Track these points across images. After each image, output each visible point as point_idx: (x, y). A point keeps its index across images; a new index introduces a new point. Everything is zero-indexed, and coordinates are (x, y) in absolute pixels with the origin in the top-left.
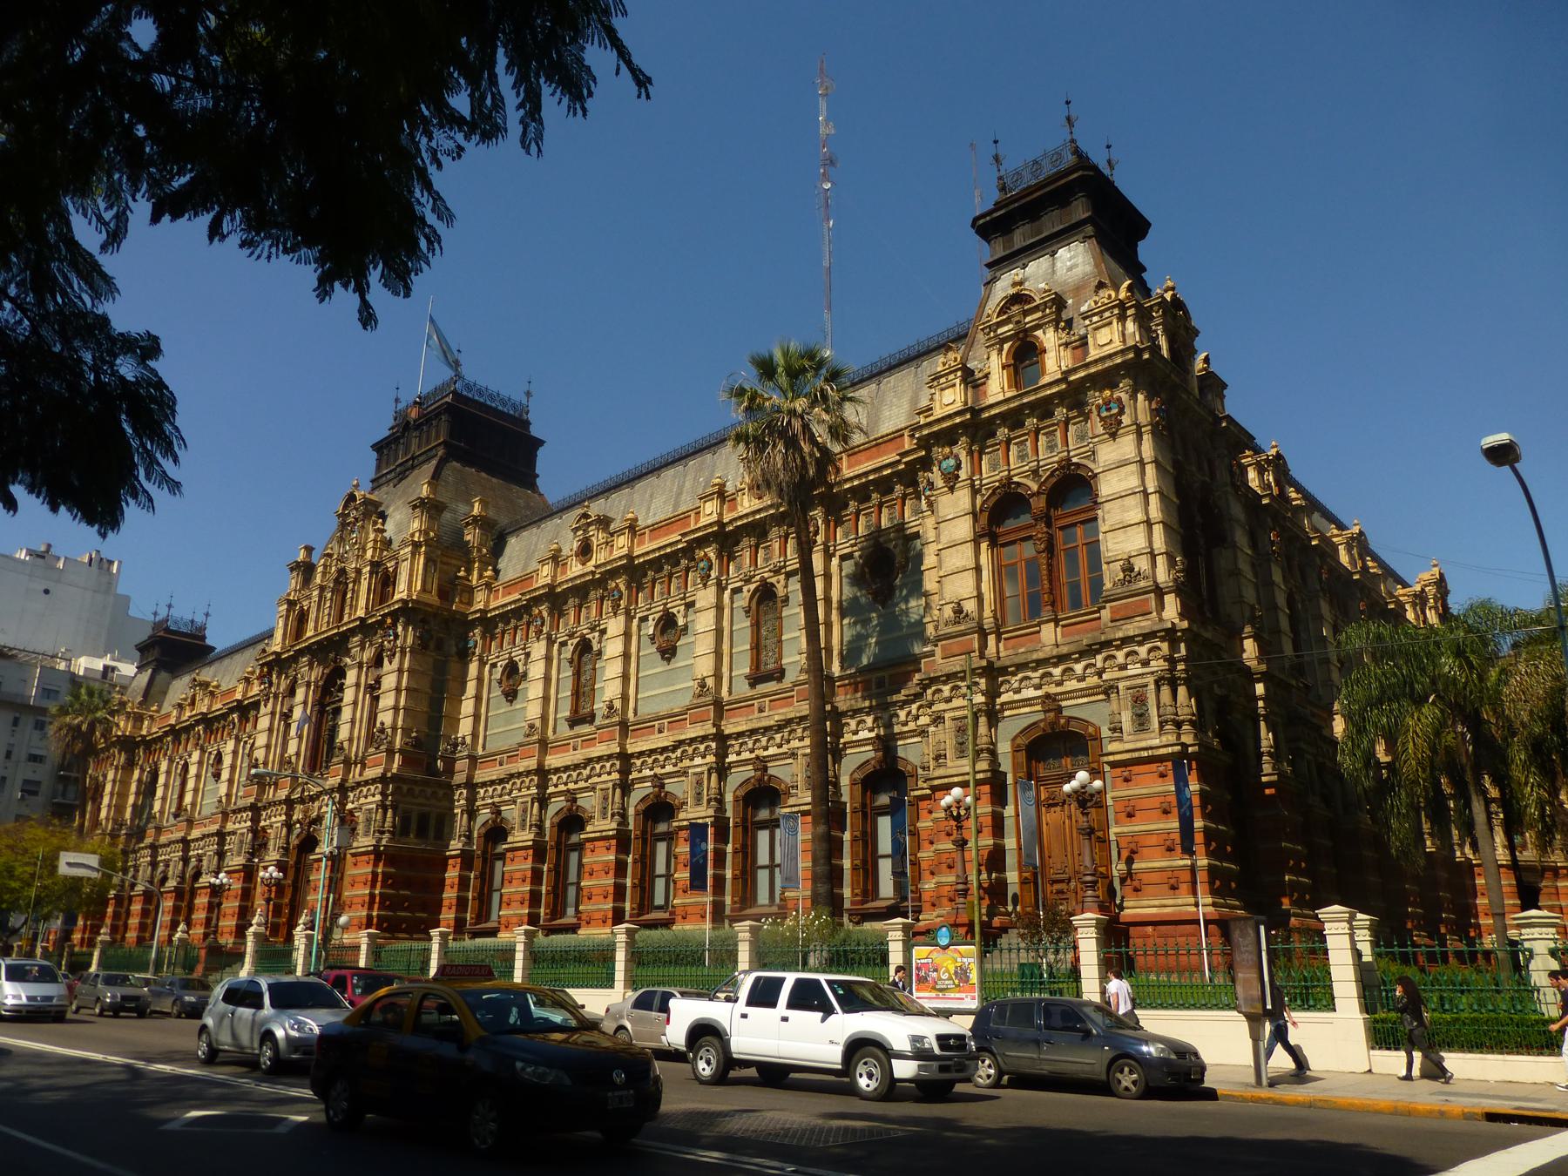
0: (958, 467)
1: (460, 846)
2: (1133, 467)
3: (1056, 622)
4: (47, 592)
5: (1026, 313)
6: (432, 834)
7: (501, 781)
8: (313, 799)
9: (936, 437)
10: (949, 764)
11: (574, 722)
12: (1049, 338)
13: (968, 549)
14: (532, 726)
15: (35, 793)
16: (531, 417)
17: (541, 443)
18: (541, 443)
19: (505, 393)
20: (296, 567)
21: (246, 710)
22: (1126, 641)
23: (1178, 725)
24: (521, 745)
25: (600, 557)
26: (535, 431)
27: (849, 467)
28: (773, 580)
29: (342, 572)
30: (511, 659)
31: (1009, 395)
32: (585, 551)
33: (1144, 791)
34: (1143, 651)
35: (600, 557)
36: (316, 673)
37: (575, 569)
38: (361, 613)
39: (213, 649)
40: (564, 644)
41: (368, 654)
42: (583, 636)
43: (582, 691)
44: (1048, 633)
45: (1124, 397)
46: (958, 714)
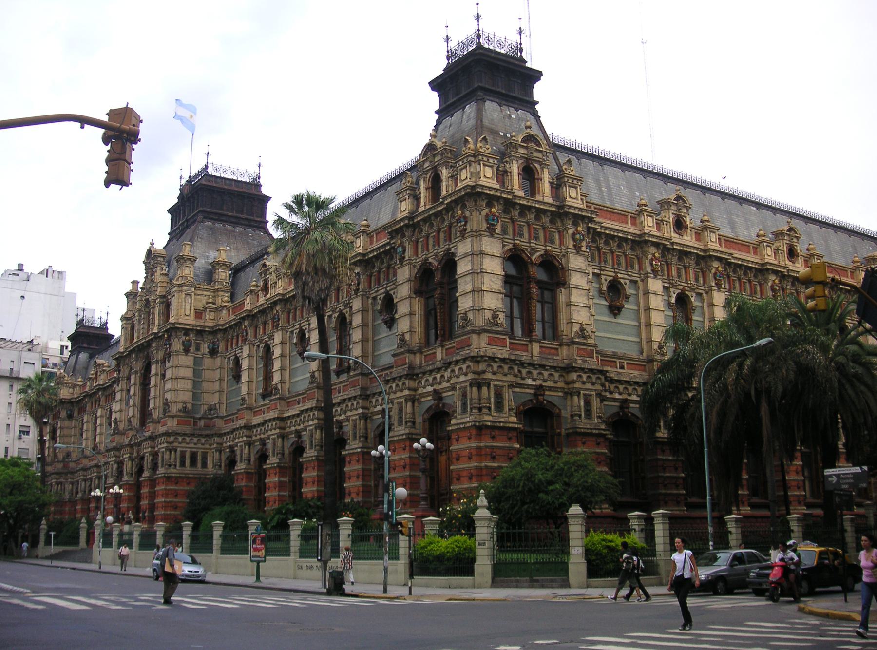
0: (404, 251)
1: (244, 467)
2: (469, 258)
3: (443, 346)
4: (23, 297)
5: (434, 156)
6: (199, 465)
7: (298, 415)
8: (139, 444)
9: (396, 230)
10: (458, 417)
11: (264, 396)
12: (445, 173)
13: (407, 302)
14: (243, 399)
15: (28, 433)
16: (262, 181)
17: (269, 198)
18: (269, 198)
19: (242, 169)
20: (128, 295)
21: (108, 391)
22: (457, 362)
23: (480, 409)
24: (239, 410)
25: (272, 293)
26: (265, 191)
27: (377, 241)
28: (344, 311)
29: (147, 301)
30: (301, 328)
31: (428, 207)
32: (265, 289)
33: (462, 447)
34: (464, 367)
35: (272, 293)
36: (138, 366)
37: (262, 300)
38: (156, 330)
39: (113, 336)
40: (258, 346)
41: (160, 355)
42: (266, 342)
43: (268, 376)
44: (439, 354)
45: (467, 214)
46: (399, 400)
